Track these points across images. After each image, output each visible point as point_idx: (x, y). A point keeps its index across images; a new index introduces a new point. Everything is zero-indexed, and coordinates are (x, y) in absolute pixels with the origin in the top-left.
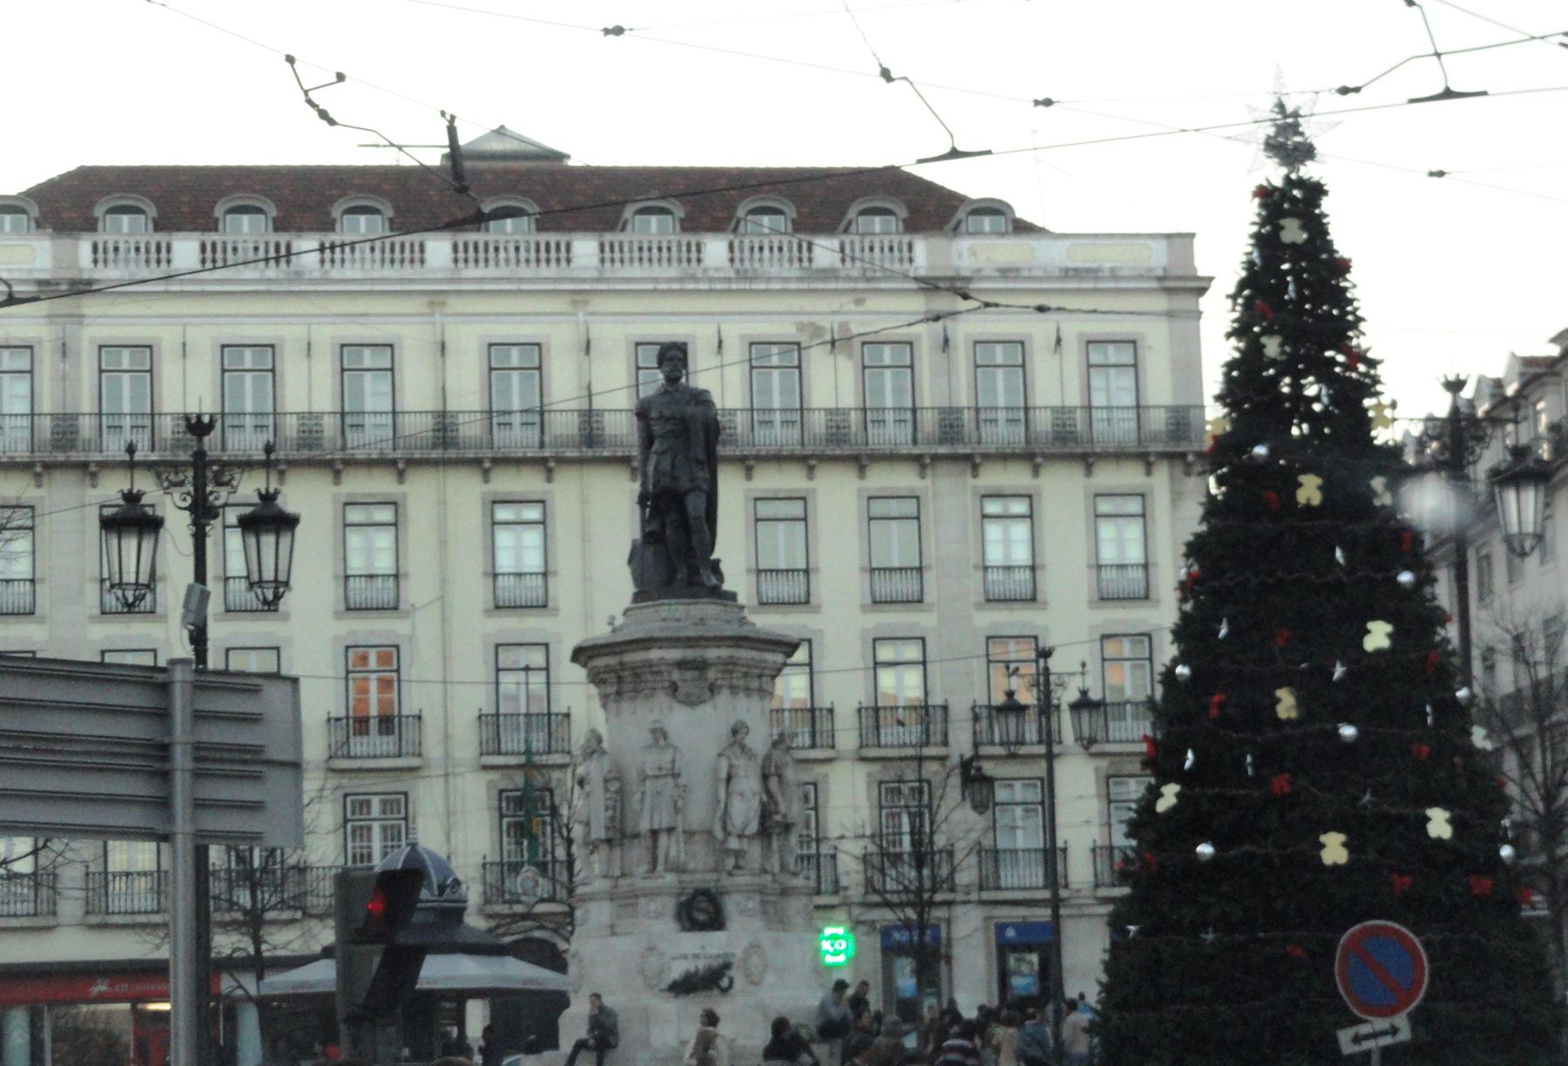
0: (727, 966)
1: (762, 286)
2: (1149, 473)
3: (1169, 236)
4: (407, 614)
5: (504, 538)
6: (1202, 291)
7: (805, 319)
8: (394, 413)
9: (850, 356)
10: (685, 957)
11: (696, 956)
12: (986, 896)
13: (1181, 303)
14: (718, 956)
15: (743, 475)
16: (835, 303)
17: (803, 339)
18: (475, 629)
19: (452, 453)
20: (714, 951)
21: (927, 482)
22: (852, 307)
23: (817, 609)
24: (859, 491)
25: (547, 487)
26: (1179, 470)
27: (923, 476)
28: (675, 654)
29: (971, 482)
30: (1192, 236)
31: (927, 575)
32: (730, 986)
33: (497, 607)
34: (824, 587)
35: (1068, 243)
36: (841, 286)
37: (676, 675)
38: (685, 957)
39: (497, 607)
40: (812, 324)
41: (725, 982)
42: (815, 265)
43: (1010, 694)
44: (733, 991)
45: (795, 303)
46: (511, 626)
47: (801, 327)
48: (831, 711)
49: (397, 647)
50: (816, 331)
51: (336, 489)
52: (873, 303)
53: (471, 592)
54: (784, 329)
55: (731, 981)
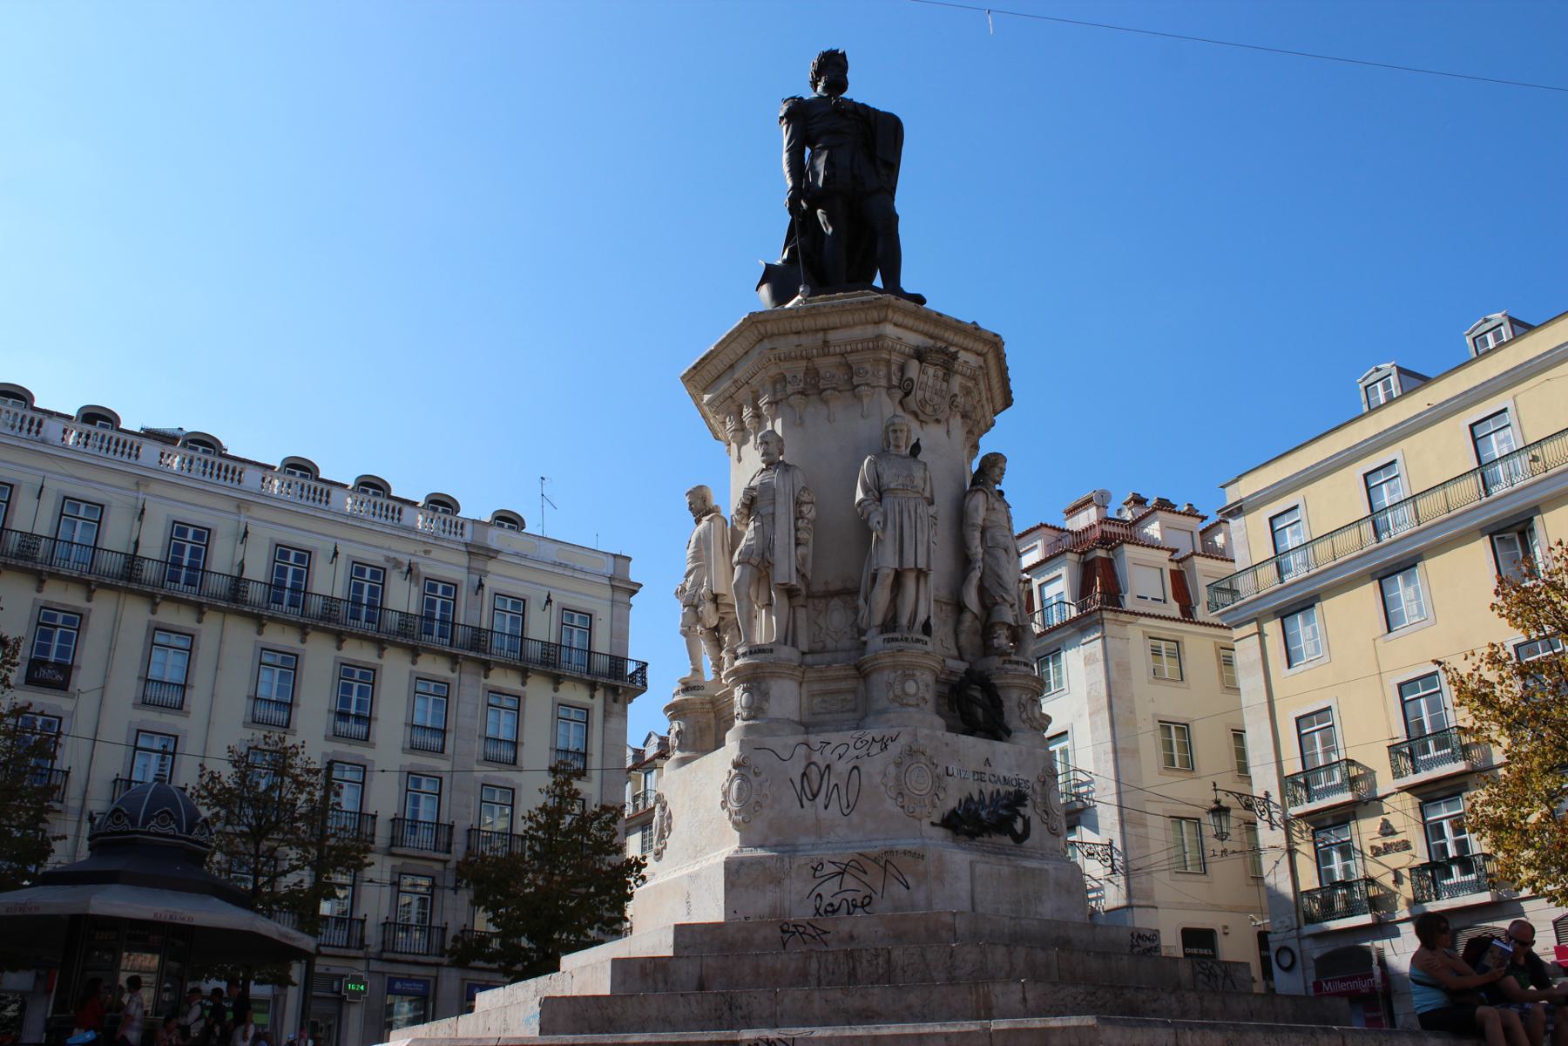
2: (592, 697)
3: (615, 556)
4: (73, 696)
5: (157, 655)
6: (635, 592)
7: (392, 555)
8: (95, 547)
9: (417, 584)
13: (619, 596)
15: (334, 644)
16: (411, 548)
17: (388, 566)
18: (123, 714)
19: (135, 586)
21: (455, 675)
23: (373, 746)
25: (198, 626)
26: (610, 698)
27: (453, 671)
29: (483, 680)
30: (629, 559)
31: (450, 738)
33: (144, 703)
35: (557, 546)
39: (144, 703)
45: (387, 543)
46: (152, 719)
48: (374, 817)
49: (60, 719)
50: (397, 564)
51: (38, 596)
53: (126, 686)
54: (375, 557)
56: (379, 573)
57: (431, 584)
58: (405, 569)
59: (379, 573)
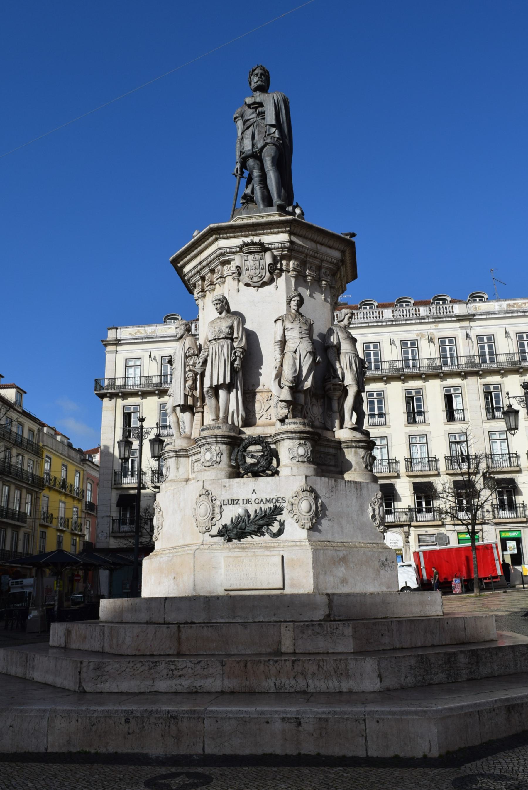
0: (277, 510)
1: (404, 322)
10: (234, 502)
11: (248, 501)
12: (495, 521)
14: (269, 501)
17: (418, 338)
20: (264, 496)
22: (435, 328)
24: (441, 385)
28: (238, 242)
32: (280, 532)
34: (429, 416)
36: (430, 320)
37: (237, 260)
38: (234, 502)
40: (421, 333)
41: (275, 527)
42: (421, 315)
43: (510, 406)
44: (282, 537)
47: (417, 335)
50: (422, 336)
52: (441, 325)
54: (411, 336)
55: (282, 524)
56: (414, 343)
57: (442, 340)
58: (427, 337)
59: (414, 343)
